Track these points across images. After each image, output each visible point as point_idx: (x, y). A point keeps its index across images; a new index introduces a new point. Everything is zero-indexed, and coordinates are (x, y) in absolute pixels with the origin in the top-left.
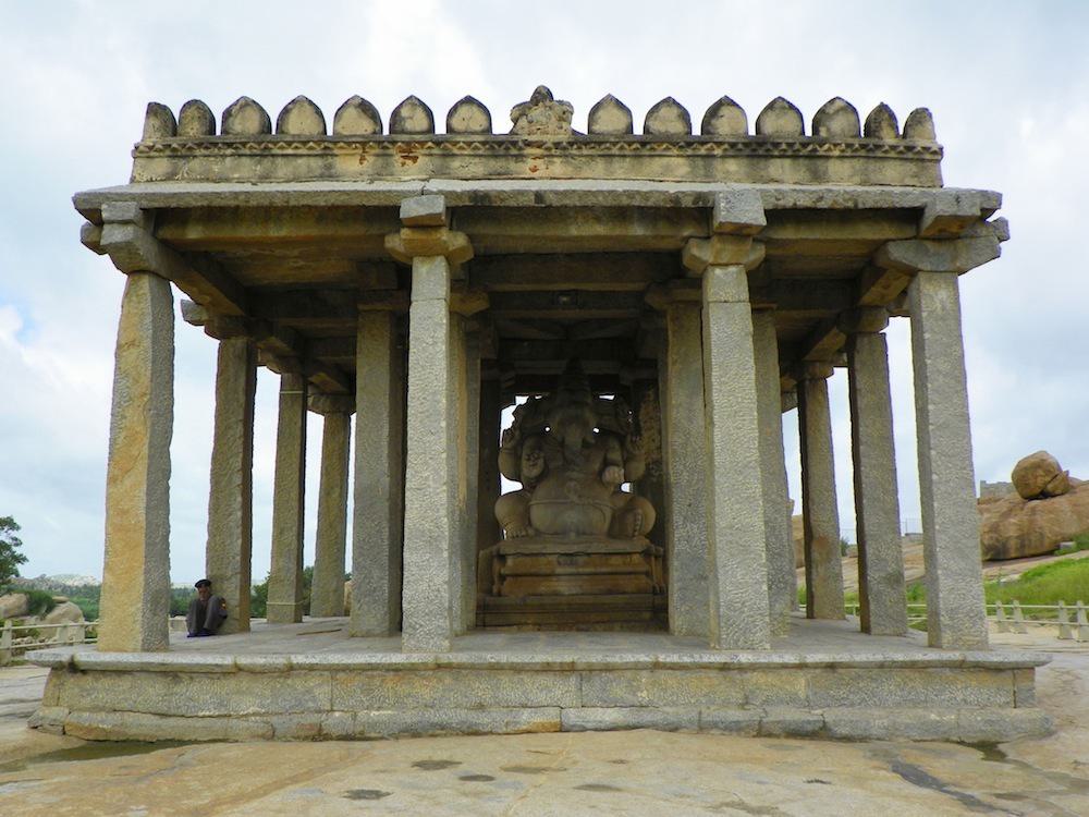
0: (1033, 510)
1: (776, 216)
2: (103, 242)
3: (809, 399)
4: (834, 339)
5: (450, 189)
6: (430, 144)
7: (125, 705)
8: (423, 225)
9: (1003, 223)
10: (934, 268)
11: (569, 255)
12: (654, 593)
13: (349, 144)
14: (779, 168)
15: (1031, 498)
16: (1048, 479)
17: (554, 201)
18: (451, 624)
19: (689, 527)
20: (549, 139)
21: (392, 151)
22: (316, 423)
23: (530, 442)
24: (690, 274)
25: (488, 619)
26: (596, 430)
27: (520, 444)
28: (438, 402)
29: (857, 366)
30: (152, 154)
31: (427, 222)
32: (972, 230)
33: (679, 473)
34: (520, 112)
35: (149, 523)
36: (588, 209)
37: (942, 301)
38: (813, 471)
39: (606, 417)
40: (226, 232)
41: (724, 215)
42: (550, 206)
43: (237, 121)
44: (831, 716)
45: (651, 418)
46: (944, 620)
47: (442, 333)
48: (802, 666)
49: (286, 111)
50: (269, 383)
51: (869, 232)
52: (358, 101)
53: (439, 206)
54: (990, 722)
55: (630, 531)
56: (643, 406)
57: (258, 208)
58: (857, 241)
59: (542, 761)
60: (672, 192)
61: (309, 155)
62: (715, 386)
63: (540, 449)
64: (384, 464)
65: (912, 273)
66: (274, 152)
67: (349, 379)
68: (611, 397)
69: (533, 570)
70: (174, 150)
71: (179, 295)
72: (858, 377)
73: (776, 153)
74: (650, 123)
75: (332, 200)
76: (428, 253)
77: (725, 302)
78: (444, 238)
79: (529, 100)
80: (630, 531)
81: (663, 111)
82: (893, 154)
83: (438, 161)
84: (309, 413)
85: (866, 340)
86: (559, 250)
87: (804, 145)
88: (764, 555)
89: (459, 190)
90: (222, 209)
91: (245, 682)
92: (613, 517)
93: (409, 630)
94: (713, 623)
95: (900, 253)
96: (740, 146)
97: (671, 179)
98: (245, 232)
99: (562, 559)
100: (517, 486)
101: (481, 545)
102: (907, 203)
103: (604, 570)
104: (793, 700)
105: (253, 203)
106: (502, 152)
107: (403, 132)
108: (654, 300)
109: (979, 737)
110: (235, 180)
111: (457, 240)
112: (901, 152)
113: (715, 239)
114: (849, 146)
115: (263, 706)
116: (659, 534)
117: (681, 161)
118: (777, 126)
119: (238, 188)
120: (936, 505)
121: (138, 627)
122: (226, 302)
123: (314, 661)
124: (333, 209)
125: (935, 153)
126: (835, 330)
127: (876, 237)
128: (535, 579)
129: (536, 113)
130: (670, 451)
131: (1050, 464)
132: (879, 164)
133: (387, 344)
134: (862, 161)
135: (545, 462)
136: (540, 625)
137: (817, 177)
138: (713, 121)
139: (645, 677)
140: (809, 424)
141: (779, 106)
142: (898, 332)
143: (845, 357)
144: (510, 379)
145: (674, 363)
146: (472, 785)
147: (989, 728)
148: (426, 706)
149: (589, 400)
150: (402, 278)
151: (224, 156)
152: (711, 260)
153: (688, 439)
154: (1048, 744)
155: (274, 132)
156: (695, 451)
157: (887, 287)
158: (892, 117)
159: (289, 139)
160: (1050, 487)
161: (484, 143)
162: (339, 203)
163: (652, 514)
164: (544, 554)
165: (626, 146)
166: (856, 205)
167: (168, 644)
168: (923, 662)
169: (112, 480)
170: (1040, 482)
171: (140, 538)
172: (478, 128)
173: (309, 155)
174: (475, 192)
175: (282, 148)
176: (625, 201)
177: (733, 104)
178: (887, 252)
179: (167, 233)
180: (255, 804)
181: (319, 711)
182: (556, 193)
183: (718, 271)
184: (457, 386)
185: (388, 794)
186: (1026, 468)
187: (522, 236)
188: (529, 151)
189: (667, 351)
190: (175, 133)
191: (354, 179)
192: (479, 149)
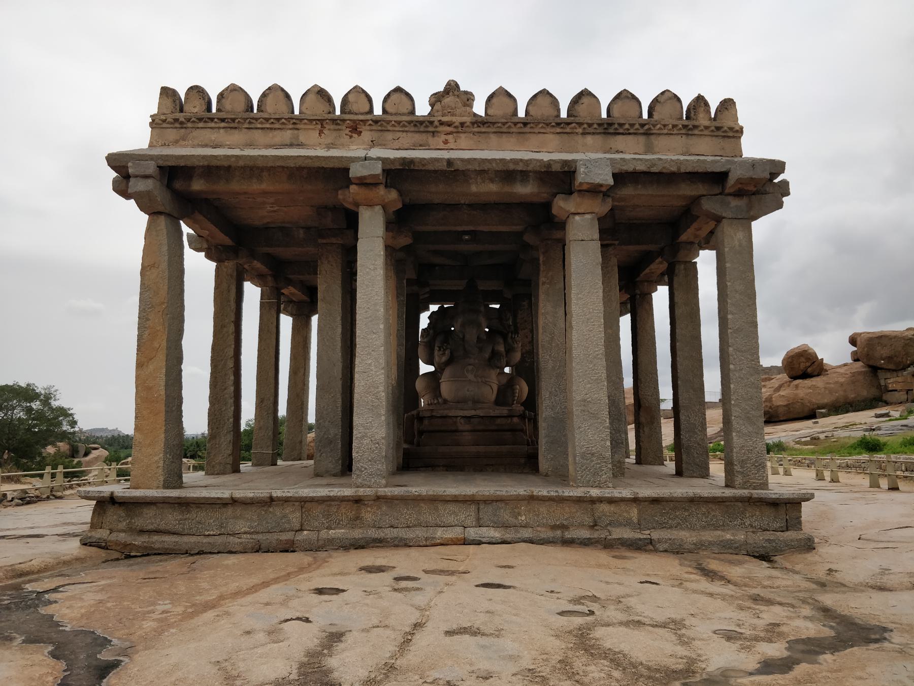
0: (797, 386)
1: (621, 178)
2: (130, 191)
4: (659, 266)
5: (386, 156)
6: (370, 122)
7: (150, 527)
8: (365, 183)
9: (785, 184)
10: (734, 216)
11: (470, 206)
13: (311, 121)
14: (619, 142)
15: (794, 378)
16: (808, 364)
20: (457, 120)
22: (286, 323)
24: (556, 220)
28: (378, 311)
29: (675, 286)
30: (165, 125)
31: (368, 181)
32: (763, 188)
33: (546, 360)
34: (436, 99)
35: (167, 396)
36: (484, 170)
38: (642, 359)
40: (221, 187)
41: (583, 177)
44: (655, 535)
46: (737, 468)
47: (380, 261)
48: (635, 500)
49: (264, 95)
50: (252, 293)
51: (688, 190)
52: (317, 90)
53: (378, 169)
54: (769, 541)
57: (244, 168)
59: (452, 566)
62: (574, 301)
64: (337, 355)
65: (718, 220)
67: (312, 292)
68: (497, 306)
70: (182, 123)
71: (186, 230)
73: (621, 131)
74: (530, 108)
75: (299, 163)
76: (370, 205)
79: (442, 90)
81: (539, 99)
82: (706, 132)
83: (375, 135)
85: (682, 267)
86: (462, 202)
87: (642, 125)
89: (392, 157)
90: (218, 168)
91: (239, 510)
93: (357, 472)
94: (571, 467)
95: (708, 205)
96: (595, 126)
97: (546, 151)
98: (236, 186)
99: (462, 421)
100: (431, 368)
101: (406, 411)
102: (718, 170)
104: (628, 523)
105: (241, 163)
106: (422, 129)
107: (350, 113)
108: (529, 238)
110: (229, 147)
111: (393, 195)
112: (712, 131)
113: (576, 194)
114: (674, 126)
117: (551, 136)
119: (230, 152)
120: (732, 386)
121: (160, 471)
123: (289, 495)
124: (300, 169)
125: (737, 131)
126: (660, 259)
129: (448, 100)
131: (810, 354)
134: (684, 136)
135: (451, 353)
137: (649, 149)
141: (625, 97)
142: (706, 263)
143: (666, 278)
145: (544, 283)
146: (404, 584)
147: (768, 545)
149: (482, 309)
150: (351, 221)
151: (219, 128)
152: (573, 210)
154: (809, 557)
155: (255, 111)
157: (700, 229)
158: (706, 104)
159: (266, 116)
160: (809, 370)
161: (410, 122)
162: (303, 165)
163: (526, 389)
165: (512, 125)
166: (679, 168)
167: (182, 482)
168: (722, 498)
169: (140, 365)
170: (802, 366)
171: (162, 407)
172: (406, 111)
174: (404, 159)
175: (261, 123)
176: (512, 167)
179: (178, 185)
180: (249, 598)
182: (462, 160)
183: (577, 218)
185: (343, 591)
187: (436, 192)
188: (441, 129)
189: (538, 274)
192: (406, 126)
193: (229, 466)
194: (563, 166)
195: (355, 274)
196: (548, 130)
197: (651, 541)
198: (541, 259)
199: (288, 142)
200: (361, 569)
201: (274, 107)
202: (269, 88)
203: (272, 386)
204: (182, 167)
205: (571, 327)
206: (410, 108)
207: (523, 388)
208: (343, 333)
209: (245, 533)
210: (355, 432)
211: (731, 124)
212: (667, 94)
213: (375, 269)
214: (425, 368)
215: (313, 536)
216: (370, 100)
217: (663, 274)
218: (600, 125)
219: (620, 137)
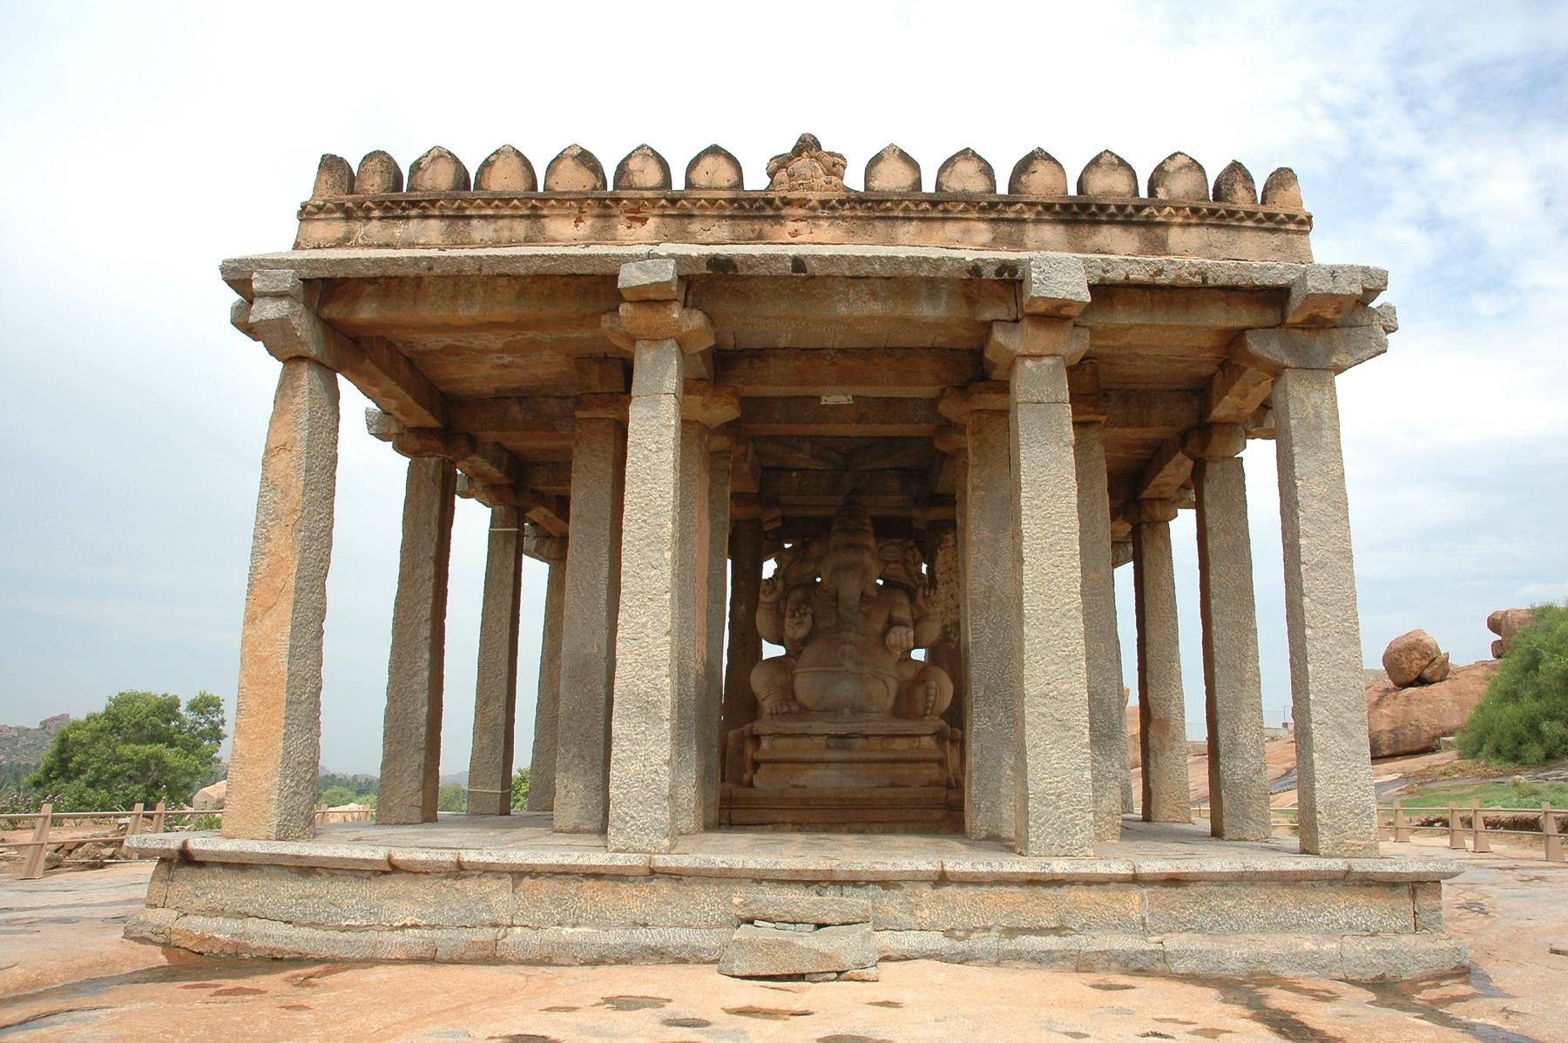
1: (1104, 292)
3: (1148, 553)
4: (1177, 469)
5: (684, 253)
8: (649, 299)
12: (949, 786)
17: (814, 267)
18: (673, 819)
21: (615, 211)
22: (535, 573)
23: (797, 595)
24: (996, 375)
25: (736, 816)
26: (880, 582)
27: (785, 596)
28: (661, 526)
29: (1207, 498)
31: (652, 296)
34: (779, 164)
36: (859, 277)
37: (1315, 406)
38: (1151, 635)
39: (892, 566)
40: (404, 313)
42: (814, 277)
43: (428, 175)
47: (669, 436)
48: (1135, 880)
49: (487, 164)
52: (576, 152)
53: (668, 273)
56: (940, 553)
58: (1209, 329)
60: (968, 259)
61: (512, 217)
65: (1276, 372)
66: (468, 213)
67: (562, 506)
69: (794, 755)
72: (1208, 511)
74: (943, 179)
75: (535, 267)
76: (656, 339)
78: (676, 315)
82: (1249, 223)
83: (673, 225)
84: (526, 559)
85: (1218, 467)
86: (829, 344)
87: (1139, 209)
88: (1087, 732)
89: (694, 254)
90: (401, 280)
92: (899, 691)
93: (618, 824)
96: (1057, 208)
97: (968, 245)
98: (430, 311)
99: (832, 742)
100: (780, 651)
104: (1122, 925)
105: (438, 271)
107: (630, 188)
108: (950, 409)
109: (1372, 974)
111: (697, 320)
113: (1025, 323)
114: (1195, 211)
115: (423, 916)
116: (957, 715)
117: (982, 226)
118: (1106, 184)
120: (1310, 667)
122: (418, 409)
123: (490, 859)
125: (1302, 222)
126: (1180, 456)
127: (1236, 323)
128: (800, 766)
132: (1232, 233)
136: (800, 824)
138: (1023, 178)
139: (926, 891)
140: (1146, 578)
144: (773, 520)
145: (975, 488)
148: (635, 923)
149: (871, 542)
151: (409, 218)
152: (1021, 350)
157: (1244, 396)
158: (1248, 178)
161: (731, 201)
162: (542, 271)
164: (809, 736)
165: (912, 206)
166: (1205, 280)
168: (1295, 873)
172: (726, 184)
173: (512, 217)
175: (479, 207)
176: (908, 270)
177: (1049, 158)
178: (1244, 345)
179: (333, 311)
181: (495, 925)
182: (820, 258)
183: (1029, 363)
186: (1399, 651)
190: (351, 192)
191: (568, 240)
193: (417, 811)
194: (999, 272)
196: (975, 215)
197: (1164, 956)
199: (521, 238)
200: (608, 1000)
201: (504, 180)
202: (497, 152)
203: (505, 675)
204: (345, 280)
206: (734, 178)
208: (610, 576)
209: (413, 926)
210: (615, 750)
211: (1291, 212)
212: (1180, 160)
214: (771, 650)
215: (534, 938)
216: (664, 166)
217: (1185, 487)
218: (1066, 207)
219: (1105, 229)
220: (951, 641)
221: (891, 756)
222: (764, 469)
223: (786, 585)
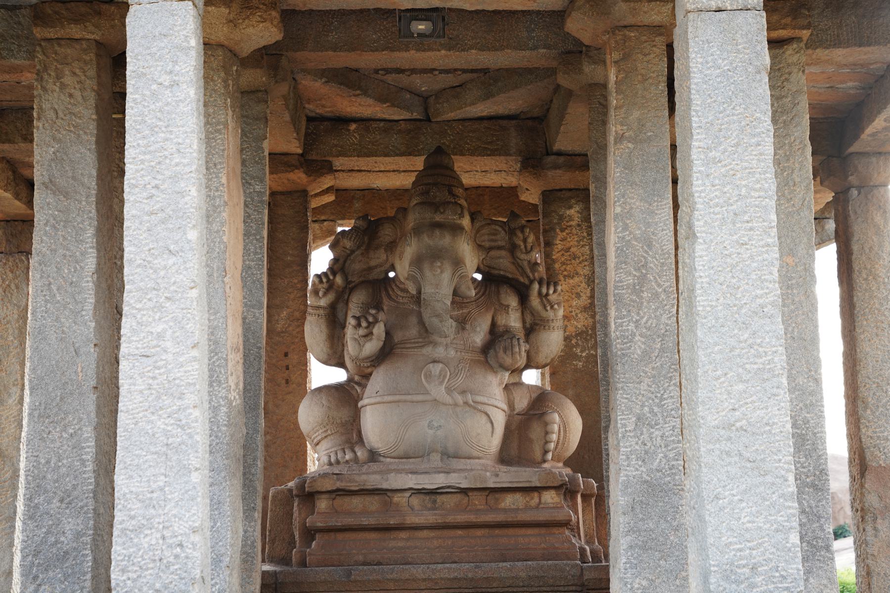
3: (857, 228)
19: (645, 436)
26: (479, 277)
28: (182, 194)
38: (865, 347)
45: (574, 259)
55: (538, 455)
56: (561, 235)
63: (379, 307)
68: (505, 220)
77: (719, 10)
80: (538, 455)
88: (791, 478)
99: (415, 501)
100: (338, 375)
103: (490, 518)
116: (591, 457)
130: (611, 299)
133: (92, 102)
135: (388, 333)
145: (620, 138)
149: (466, 222)
153: (645, 275)
156: (657, 295)
163: (576, 424)
184: (224, 180)
189: (604, 123)
195: (121, 96)
198: (612, 78)
205: (692, 236)
207: (568, 424)
210: (119, 516)
213: (174, 84)
220: (578, 358)
221: (500, 518)
222: (310, 119)
223: (347, 282)
